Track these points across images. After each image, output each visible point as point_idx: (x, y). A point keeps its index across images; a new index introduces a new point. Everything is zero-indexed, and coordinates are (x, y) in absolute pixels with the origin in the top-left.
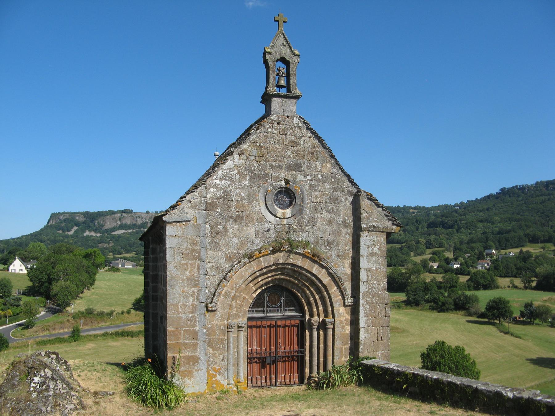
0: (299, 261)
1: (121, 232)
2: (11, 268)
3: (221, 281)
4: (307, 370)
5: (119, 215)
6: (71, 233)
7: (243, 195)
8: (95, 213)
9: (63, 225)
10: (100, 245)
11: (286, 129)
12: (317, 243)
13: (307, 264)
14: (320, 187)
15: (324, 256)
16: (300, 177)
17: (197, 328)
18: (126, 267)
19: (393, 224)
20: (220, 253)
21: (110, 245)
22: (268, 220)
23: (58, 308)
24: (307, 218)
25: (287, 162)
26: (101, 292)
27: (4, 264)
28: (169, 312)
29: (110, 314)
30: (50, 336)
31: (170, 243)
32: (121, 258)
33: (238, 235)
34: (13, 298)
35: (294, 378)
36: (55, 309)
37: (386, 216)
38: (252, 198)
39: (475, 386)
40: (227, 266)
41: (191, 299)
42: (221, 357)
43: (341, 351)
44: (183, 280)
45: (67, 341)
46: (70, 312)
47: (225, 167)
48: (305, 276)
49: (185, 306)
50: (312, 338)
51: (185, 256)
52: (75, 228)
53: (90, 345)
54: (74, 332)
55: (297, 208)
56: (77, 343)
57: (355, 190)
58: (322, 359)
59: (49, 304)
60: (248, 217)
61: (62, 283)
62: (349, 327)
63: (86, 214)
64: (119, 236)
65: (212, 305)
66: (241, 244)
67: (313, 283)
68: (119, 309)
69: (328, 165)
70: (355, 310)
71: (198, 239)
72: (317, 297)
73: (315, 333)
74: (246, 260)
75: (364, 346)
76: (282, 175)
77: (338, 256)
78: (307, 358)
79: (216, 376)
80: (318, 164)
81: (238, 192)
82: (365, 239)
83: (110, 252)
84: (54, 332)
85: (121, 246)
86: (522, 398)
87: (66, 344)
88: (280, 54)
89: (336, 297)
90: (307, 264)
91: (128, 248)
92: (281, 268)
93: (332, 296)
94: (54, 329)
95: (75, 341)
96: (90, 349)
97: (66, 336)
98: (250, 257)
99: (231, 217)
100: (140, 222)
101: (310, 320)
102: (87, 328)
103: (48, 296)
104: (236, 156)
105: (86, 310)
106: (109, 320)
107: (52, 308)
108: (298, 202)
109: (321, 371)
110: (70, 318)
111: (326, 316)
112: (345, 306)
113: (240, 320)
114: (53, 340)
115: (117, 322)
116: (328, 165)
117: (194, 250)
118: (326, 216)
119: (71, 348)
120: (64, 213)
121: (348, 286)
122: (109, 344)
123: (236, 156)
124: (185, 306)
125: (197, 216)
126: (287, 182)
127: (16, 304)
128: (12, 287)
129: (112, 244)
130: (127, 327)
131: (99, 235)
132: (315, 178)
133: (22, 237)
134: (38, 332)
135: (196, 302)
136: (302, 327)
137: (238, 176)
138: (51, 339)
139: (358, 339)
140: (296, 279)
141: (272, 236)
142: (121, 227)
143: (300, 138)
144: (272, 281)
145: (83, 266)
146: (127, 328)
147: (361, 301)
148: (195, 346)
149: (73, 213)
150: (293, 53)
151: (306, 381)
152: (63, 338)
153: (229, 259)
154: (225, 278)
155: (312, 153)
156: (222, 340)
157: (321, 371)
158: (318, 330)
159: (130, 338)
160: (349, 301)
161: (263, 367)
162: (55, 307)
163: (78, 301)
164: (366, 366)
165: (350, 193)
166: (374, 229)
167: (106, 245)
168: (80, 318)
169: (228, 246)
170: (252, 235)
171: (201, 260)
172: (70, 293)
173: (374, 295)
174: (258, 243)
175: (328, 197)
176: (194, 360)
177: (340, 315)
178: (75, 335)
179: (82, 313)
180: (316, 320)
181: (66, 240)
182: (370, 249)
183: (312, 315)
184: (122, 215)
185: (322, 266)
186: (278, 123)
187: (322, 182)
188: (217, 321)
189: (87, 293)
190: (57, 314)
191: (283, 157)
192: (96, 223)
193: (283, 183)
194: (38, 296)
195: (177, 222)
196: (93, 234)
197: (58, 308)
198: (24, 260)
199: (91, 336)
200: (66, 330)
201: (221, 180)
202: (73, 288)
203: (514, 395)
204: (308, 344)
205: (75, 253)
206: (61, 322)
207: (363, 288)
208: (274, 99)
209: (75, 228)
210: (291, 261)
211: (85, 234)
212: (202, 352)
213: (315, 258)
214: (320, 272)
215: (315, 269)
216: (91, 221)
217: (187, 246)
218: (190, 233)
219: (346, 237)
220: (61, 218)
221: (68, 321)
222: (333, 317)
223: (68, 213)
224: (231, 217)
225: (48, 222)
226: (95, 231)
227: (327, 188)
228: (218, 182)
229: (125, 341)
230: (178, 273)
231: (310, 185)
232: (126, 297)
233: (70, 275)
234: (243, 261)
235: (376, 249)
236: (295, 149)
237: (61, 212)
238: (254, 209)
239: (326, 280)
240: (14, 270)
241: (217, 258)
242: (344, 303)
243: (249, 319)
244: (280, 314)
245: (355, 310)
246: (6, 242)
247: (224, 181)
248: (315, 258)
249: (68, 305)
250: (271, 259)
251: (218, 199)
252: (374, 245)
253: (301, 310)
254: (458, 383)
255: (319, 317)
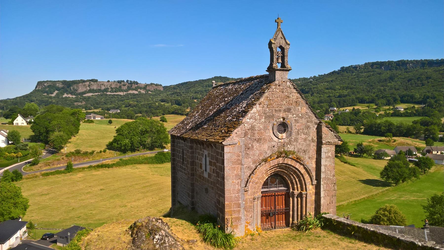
0: (290, 162)
1: (90, 94)
2: (15, 122)
3: (251, 175)
4: (291, 219)
5: (88, 83)
6: (53, 95)
7: (261, 127)
8: (70, 81)
9: (47, 89)
10: (75, 103)
11: (283, 89)
12: (299, 151)
13: (293, 163)
14: (301, 121)
15: (302, 159)
16: (290, 116)
17: (240, 202)
18: (96, 119)
19: (339, 140)
20: (250, 159)
21: (83, 103)
22: (274, 140)
23: (55, 150)
24: (293, 138)
25: (284, 107)
26: (84, 138)
27: (7, 117)
28: (226, 194)
29: (92, 153)
30: (51, 169)
31: (226, 156)
32: (92, 113)
33: (259, 149)
34: (22, 144)
35: (283, 223)
36: (52, 151)
37: (335, 136)
38: (266, 128)
39: (398, 237)
40: (254, 167)
41: (237, 186)
42: (250, 216)
43: (310, 209)
44: (233, 176)
45: (64, 173)
46: (64, 153)
47: (252, 112)
48: (292, 169)
49: (234, 190)
50: (294, 202)
51: (234, 163)
52: (56, 92)
53: (80, 175)
54: (68, 166)
55: (289, 133)
56: (71, 173)
57: (319, 122)
58: (299, 214)
59: (47, 147)
60: (264, 139)
61: (56, 133)
62: (314, 196)
63: (64, 82)
64: (89, 97)
65: (246, 188)
66: (261, 154)
67: (295, 172)
68: (97, 150)
69: (305, 108)
70: (318, 188)
71: (240, 154)
72: (297, 180)
73: (296, 199)
74: (264, 163)
75: (323, 207)
76: (281, 115)
77: (309, 158)
78: (291, 213)
79: (248, 226)
80: (299, 108)
81: (259, 126)
82: (324, 149)
83: (83, 108)
84: (53, 167)
85: (91, 104)
86: (427, 246)
87: (63, 174)
88: (280, 44)
89: (308, 180)
90: (293, 163)
91: (96, 105)
92: (279, 166)
93: (306, 179)
94: (53, 165)
95: (69, 172)
96: (80, 178)
97: (63, 169)
98: (265, 160)
99: (255, 140)
100: (103, 88)
101: (293, 193)
102: (76, 163)
103: (46, 142)
104: (258, 106)
105: (75, 151)
106: (91, 157)
107: (50, 150)
108: (289, 130)
109: (299, 219)
110: (64, 157)
111: (302, 190)
112: (312, 185)
113: (258, 194)
114: (53, 172)
115: (97, 158)
116: (305, 108)
117: (239, 160)
118: (303, 136)
119: (67, 177)
120: (48, 81)
121: (314, 174)
122: (93, 173)
123: (258, 106)
124: (234, 190)
125: (240, 141)
126: (284, 119)
127: (24, 148)
128: (20, 137)
129: (84, 103)
130: (104, 161)
131: (74, 97)
132: (298, 116)
133: (17, 98)
134: (42, 167)
135: (240, 188)
136: (288, 195)
137: (259, 117)
138: (52, 171)
139: (320, 203)
140: (286, 170)
141: (276, 149)
142: (90, 91)
143: (290, 94)
144: (273, 172)
145: (71, 121)
146: (105, 162)
147: (322, 183)
148: (239, 211)
149: (54, 81)
150: (287, 43)
151: (290, 225)
152: (61, 171)
153: (254, 162)
154: (252, 173)
155: (297, 102)
156: (251, 206)
157: (299, 219)
158: (297, 198)
159: (107, 168)
160: (315, 182)
161: (267, 218)
162: (51, 149)
163: (68, 145)
164: (326, 218)
165: (316, 123)
166: (329, 143)
167: (80, 104)
168: (71, 156)
169: (254, 155)
170: (264, 149)
171: (242, 165)
172: (63, 139)
173: (329, 179)
174: (269, 153)
175: (304, 126)
176: (239, 219)
177: (310, 190)
178: (69, 169)
179: (73, 153)
180: (296, 192)
181: (50, 100)
182: (327, 154)
183: (294, 189)
184: (90, 83)
185: (301, 164)
186: (279, 86)
187: (302, 118)
188: (249, 196)
189: (73, 139)
190: (54, 155)
191: (281, 105)
192: (72, 89)
193: (282, 119)
194: (39, 142)
195: (230, 145)
196: (70, 96)
197: (55, 150)
198: (25, 116)
199: (80, 168)
200: (62, 165)
201: (250, 119)
202: (65, 137)
203: (422, 245)
204: (291, 205)
205: (63, 112)
206: (58, 160)
207: (323, 176)
208: (277, 72)
209: (56, 92)
210: (286, 162)
211: (64, 96)
212: (242, 215)
213: (298, 160)
214: (300, 167)
215: (298, 166)
216: (68, 87)
217: (235, 157)
218: (236, 150)
219: (313, 147)
220: (46, 84)
221: (63, 159)
222: (306, 191)
223: (50, 81)
224: (255, 140)
225: (36, 88)
226: (71, 93)
227: (304, 121)
228: (248, 120)
229: (103, 171)
230: (230, 172)
231: (295, 120)
232: (101, 141)
233: (63, 127)
234: (262, 163)
235: (330, 154)
236: (288, 100)
237: (45, 81)
238: (267, 134)
239: (303, 171)
240: (17, 124)
241: (249, 163)
242: (312, 183)
243: (262, 192)
244: (276, 189)
245: (318, 188)
246: (5, 101)
247: (251, 120)
248: (298, 160)
249: (62, 148)
250: (276, 162)
251: (248, 130)
252: (328, 152)
253: (287, 186)
254: (387, 234)
255: (298, 190)
